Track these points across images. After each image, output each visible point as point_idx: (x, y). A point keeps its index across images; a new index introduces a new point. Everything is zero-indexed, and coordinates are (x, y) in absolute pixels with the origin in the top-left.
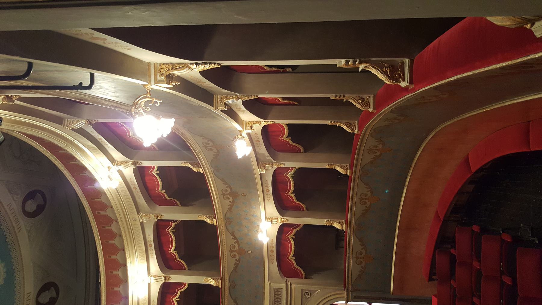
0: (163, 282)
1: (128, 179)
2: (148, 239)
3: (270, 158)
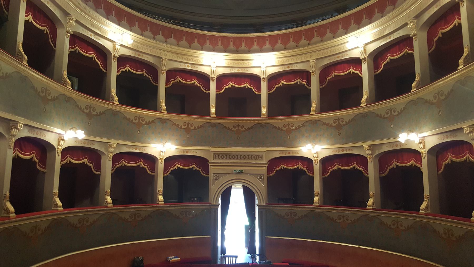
0: (262, 77)
1: (348, 53)
2: (294, 65)
3: (377, 153)
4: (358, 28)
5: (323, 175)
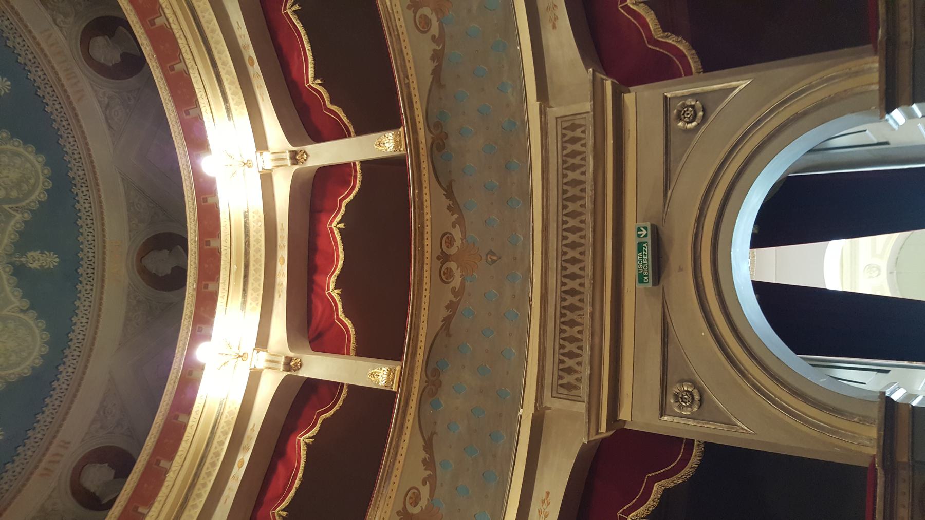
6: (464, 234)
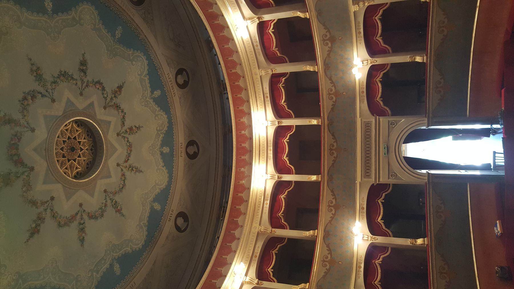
0: (277, 125)
1: (252, 36)
2: (265, 92)
4: (228, 27)
5: (389, 53)
6: (337, 144)
